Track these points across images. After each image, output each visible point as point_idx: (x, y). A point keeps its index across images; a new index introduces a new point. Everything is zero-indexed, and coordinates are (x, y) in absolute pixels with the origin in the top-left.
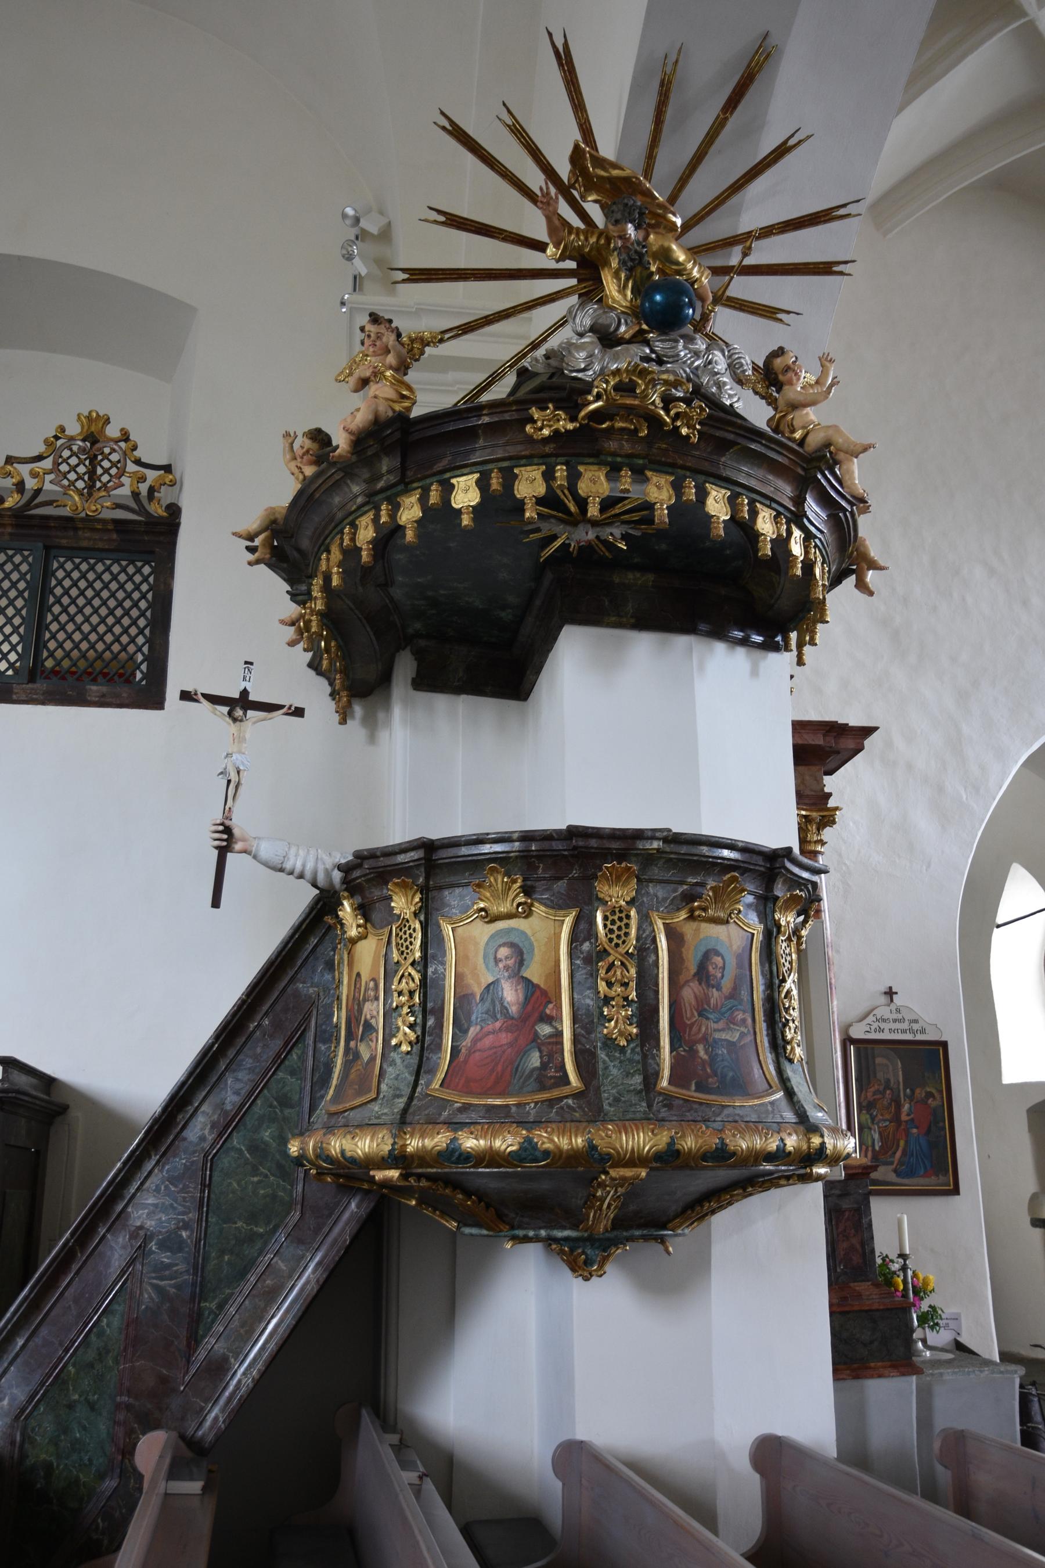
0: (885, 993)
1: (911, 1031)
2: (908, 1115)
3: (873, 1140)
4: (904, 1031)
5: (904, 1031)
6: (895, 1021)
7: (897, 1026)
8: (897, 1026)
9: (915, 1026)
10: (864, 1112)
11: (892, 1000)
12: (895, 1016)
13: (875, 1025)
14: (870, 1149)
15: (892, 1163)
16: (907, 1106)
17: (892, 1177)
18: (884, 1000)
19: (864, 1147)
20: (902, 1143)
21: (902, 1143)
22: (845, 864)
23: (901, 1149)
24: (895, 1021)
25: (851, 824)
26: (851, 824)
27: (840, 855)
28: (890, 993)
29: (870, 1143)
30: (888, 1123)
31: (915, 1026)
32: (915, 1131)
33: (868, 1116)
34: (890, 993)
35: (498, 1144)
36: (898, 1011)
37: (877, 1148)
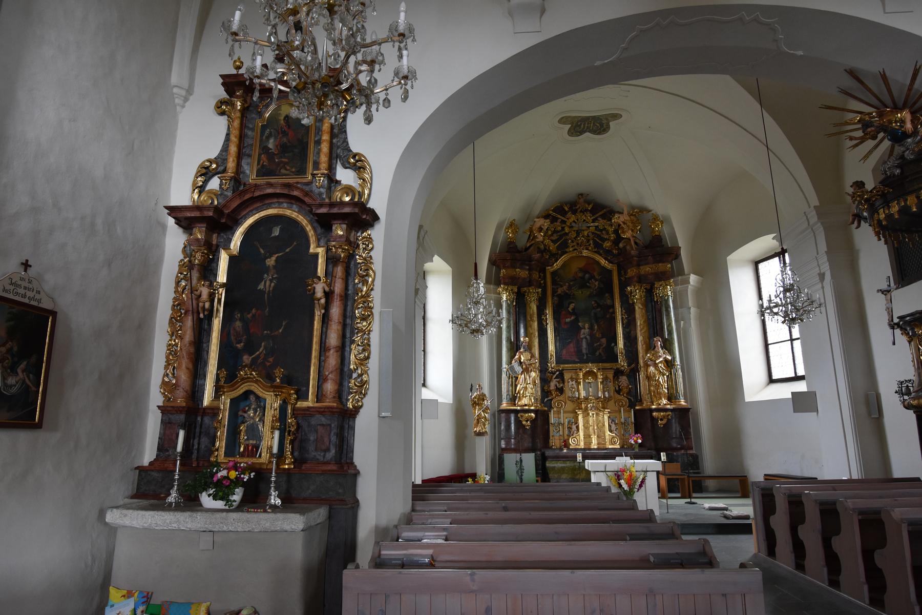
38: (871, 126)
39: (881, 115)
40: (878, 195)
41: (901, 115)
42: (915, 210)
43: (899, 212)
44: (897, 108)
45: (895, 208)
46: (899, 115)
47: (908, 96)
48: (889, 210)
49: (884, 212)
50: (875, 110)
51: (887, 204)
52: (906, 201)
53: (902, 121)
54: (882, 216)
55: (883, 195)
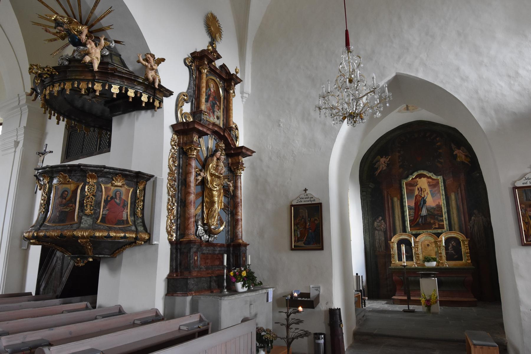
0: (304, 190)
1: (311, 201)
2: (309, 226)
3: (298, 234)
4: (308, 201)
5: (308, 201)
6: (306, 198)
7: (307, 200)
8: (307, 200)
9: (312, 199)
10: (295, 226)
11: (306, 192)
12: (306, 197)
13: (300, 200)
14: (297, 237)
15: (303, 241)
16: (308, 223)
17: (303, 245)
18: (304, 192)
19: (295, 236)
20: (306, 235)
21: (306, 235)
22: (294, 154)
23: (306, 236)
24: (306, 198)
25: (297, 141)
26: (297, 141)
27: (293, 151)
28: (306, 190)
29: (297, 235)
30: (302, 229)
31: (312, 199)
32: (311, 231)
33: (296, 227)
34: (306, 190)
35: (114, 234)
36: (307, 195)
37: (299, 236)
38: (61, 26)
39: (70, 22)
40: (48, 74)
41: (82, 28)
42: (68, 93)
43: (58, 91)
44: (81, 23)
45: (56, 89)
46: (80, 27)
47: (90, 17)
48: (53, 88)
49: (49, 89)
50: (67, 16)
51: (52, 84)
52: (65, 84)
53: (81, 33)
54: (48, 92)
55: (52, 76)
